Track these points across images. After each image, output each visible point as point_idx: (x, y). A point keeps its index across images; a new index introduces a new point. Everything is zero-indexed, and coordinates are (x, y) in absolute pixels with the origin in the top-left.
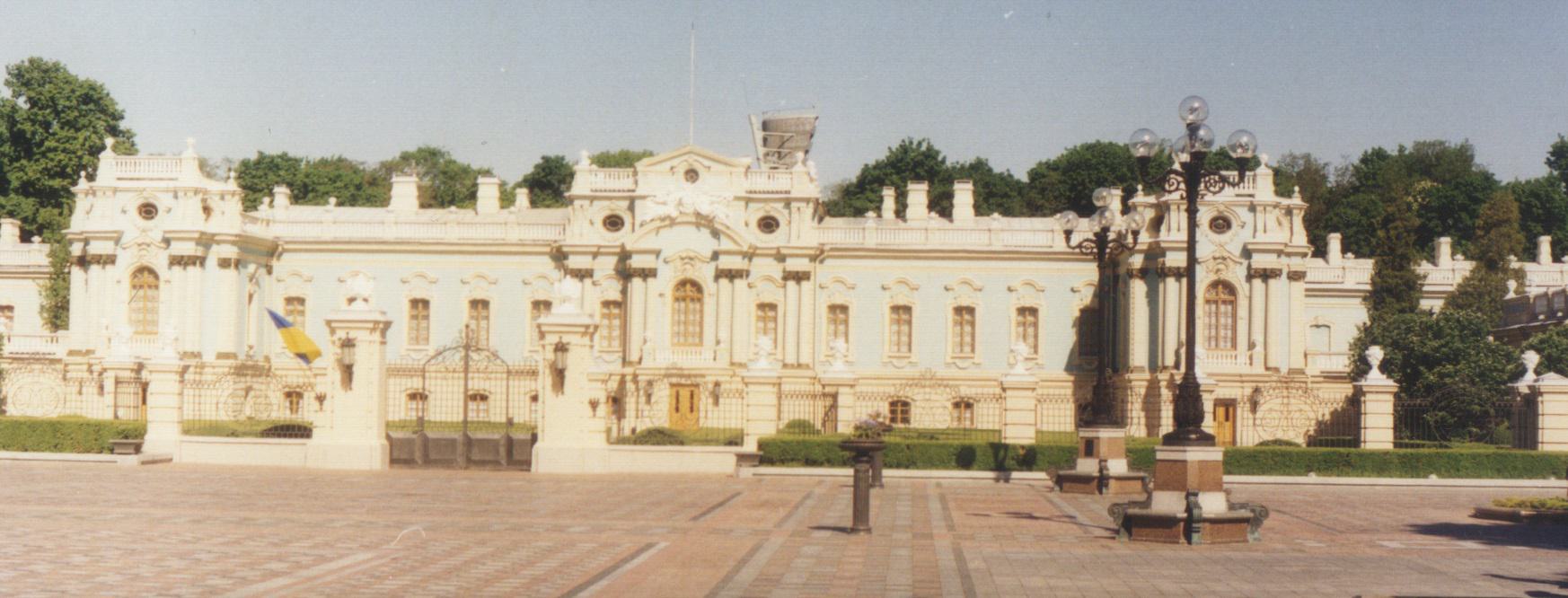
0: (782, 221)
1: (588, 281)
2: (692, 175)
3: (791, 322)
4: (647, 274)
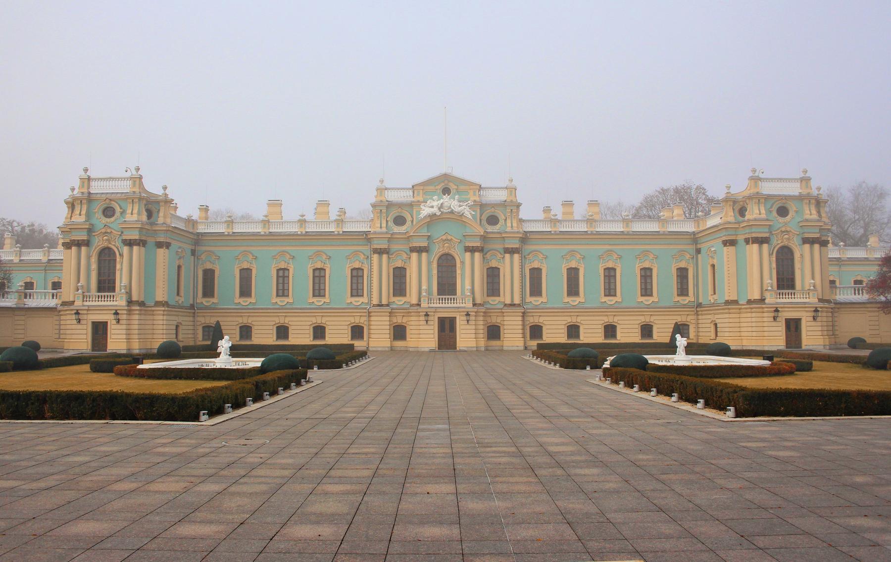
0: (501, 218)
1: (385, 256)
2: (446, 191)
3: (508, 276)
4: (420, 250)
